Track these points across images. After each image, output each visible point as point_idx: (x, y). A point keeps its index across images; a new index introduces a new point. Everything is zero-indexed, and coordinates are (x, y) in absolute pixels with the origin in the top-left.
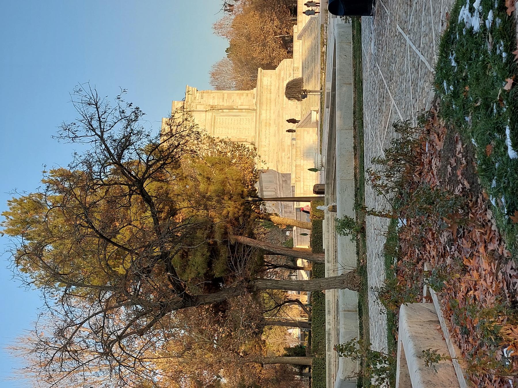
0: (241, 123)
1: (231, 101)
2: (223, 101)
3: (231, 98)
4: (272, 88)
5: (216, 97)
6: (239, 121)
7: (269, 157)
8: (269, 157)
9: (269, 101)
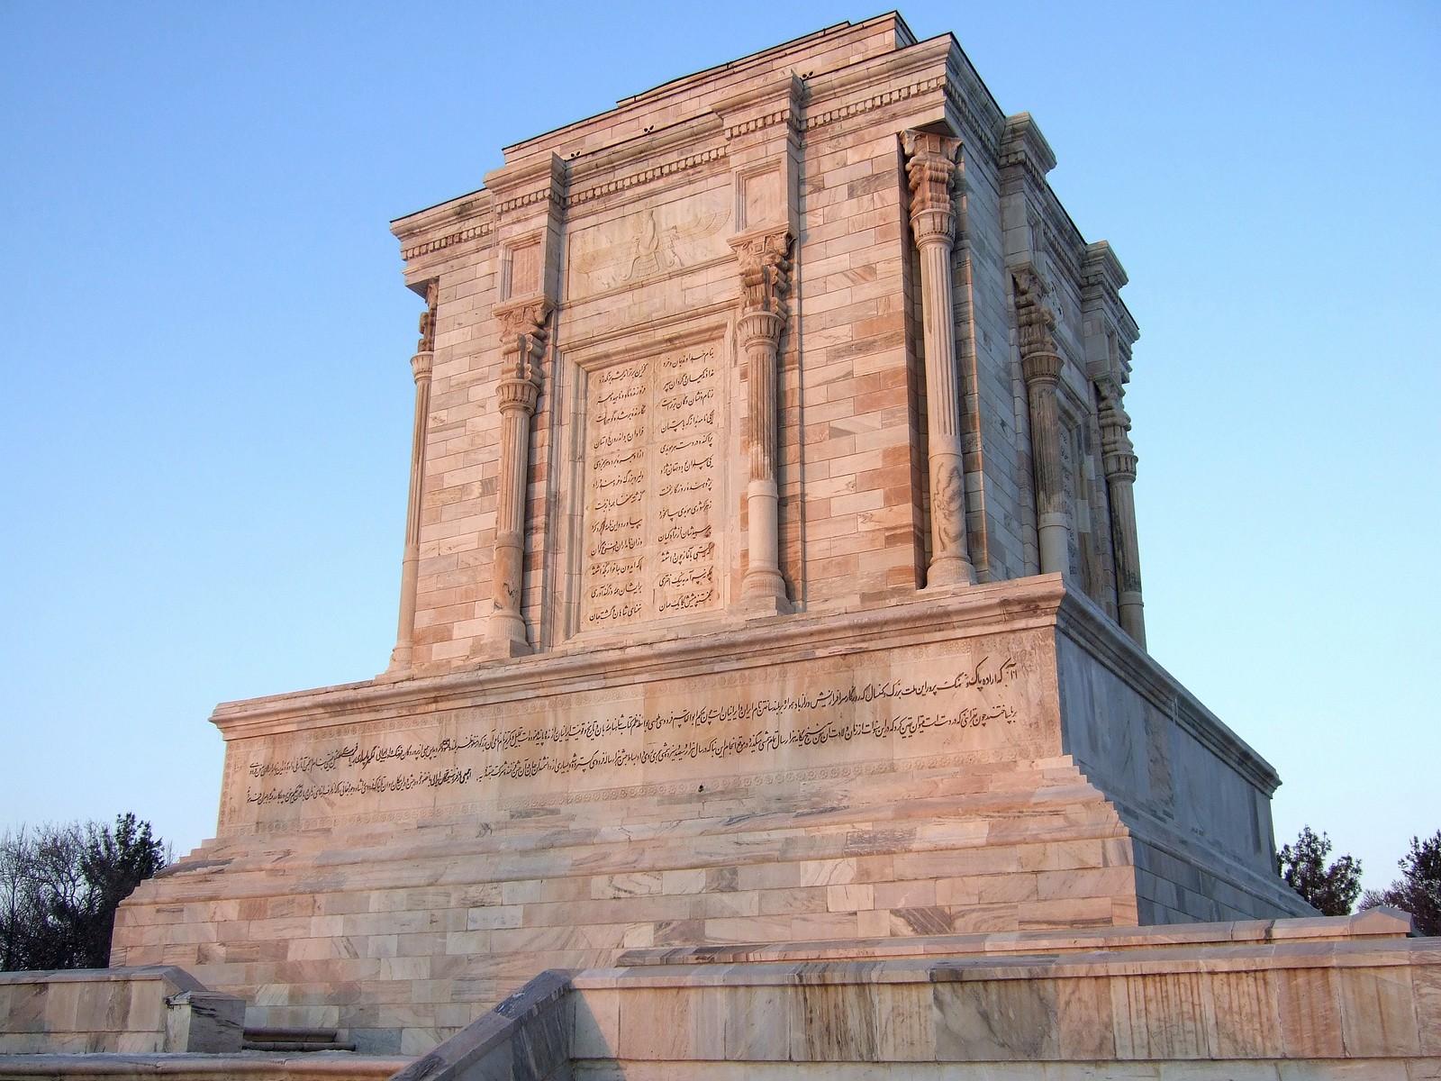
0: (677, 547)
1: (841, 415)
2: (837, 354)
3: (864, 407)
4: (863, 750)
5: (869, 290)
6: (685, 523)
7: (292, 797)
8: (292, 797)
9: (733, 729)
